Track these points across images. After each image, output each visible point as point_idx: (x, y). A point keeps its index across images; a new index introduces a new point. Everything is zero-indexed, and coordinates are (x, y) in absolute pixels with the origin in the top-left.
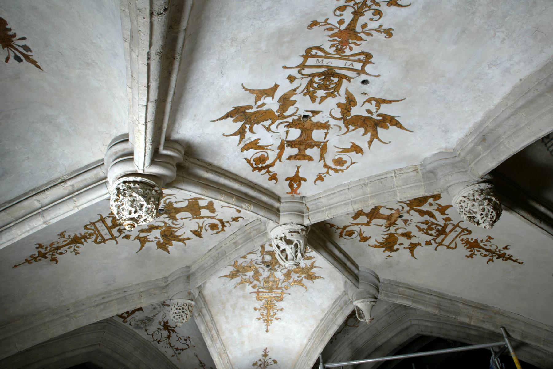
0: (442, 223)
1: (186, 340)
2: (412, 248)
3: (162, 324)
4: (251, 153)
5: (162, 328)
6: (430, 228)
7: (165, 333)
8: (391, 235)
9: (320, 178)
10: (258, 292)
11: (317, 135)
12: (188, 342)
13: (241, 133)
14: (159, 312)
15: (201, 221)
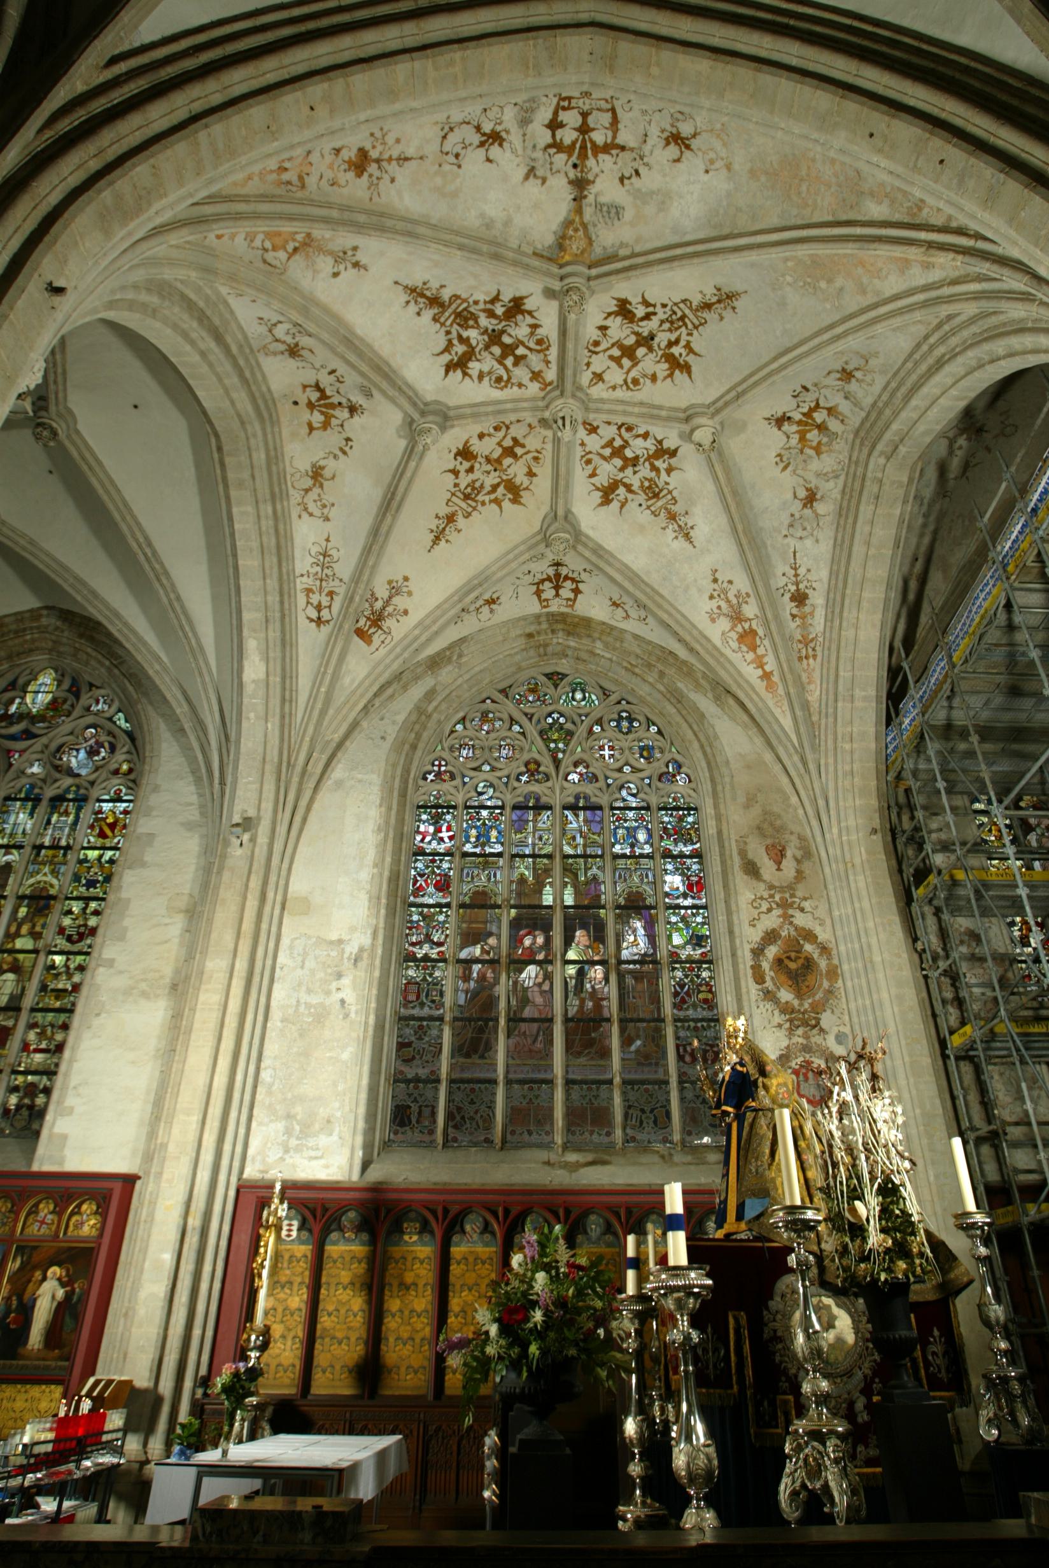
0: (480, 498)
1: (457, 156)
2: (455, 472)
3: (504, 134)
4: (641, 431)
5: (498, 128)
6: (474, 489)
7: (487, 128)
8: (475, 457)
9: (583, 444)
10: (465, 301)
11: (618, 462)
12: (452, 159)
13: (660, 442)
14: (524, 148)
15: (611, 341)
